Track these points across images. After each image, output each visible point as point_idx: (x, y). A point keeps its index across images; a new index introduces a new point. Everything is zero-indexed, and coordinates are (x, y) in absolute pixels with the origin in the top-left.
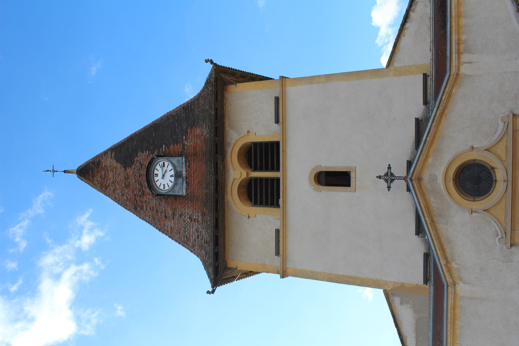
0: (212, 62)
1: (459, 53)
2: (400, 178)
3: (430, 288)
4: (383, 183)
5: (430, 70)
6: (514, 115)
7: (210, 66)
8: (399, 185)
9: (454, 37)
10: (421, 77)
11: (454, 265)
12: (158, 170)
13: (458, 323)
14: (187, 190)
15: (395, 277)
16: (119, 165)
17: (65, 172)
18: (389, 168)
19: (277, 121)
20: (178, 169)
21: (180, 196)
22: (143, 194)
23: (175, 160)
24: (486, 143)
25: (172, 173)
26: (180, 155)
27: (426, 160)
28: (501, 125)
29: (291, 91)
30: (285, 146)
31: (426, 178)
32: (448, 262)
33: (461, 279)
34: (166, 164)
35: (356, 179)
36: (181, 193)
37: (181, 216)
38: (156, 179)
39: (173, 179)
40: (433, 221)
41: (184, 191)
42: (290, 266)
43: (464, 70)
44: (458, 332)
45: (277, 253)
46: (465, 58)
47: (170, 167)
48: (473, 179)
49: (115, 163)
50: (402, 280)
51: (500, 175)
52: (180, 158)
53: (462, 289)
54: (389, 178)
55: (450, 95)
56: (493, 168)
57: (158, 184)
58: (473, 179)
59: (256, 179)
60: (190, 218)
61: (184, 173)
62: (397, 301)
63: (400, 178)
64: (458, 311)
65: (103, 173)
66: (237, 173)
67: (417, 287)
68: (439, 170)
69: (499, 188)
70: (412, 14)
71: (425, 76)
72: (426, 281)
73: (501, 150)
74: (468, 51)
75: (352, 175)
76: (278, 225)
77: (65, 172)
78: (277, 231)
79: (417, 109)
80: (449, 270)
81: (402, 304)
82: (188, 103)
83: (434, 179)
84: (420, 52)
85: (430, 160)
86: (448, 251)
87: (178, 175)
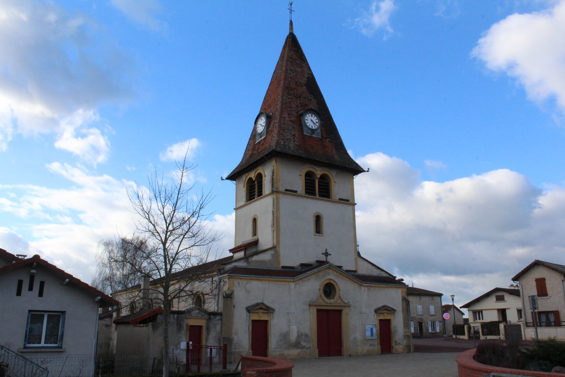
0: (368, 171)
1: (368, 286)
2: (326, 259)
3: (279, 268)
4: (329, 252)
5: (357, 273)
6: (349, 306)
7: (366, 170)
8: (323, 258)
9: (373, 285)
10: (354, 269)
11: (300, 282)
12: (315, 119)
13: (280, 283)
14: (307, 136)
15: (283, 251)
16: (306, 80)
17: (291, 21)
18: (330, 255)
19: (340, 199)
20: (315, 132)
21: (302, 129)
22: (297, 98)
23: (319, 131)
24: (341, 296)
25: (314, 128)
26: (322, 136)
27: (335, 271)
28: (346, 301)
29: (350, 207)
30: (328, 201)
31: (330, 271)
32: (301, 279)
33: (296, 284)
34: (317, 124)
35: (319, 237)
36: (304, 131)
37: (293, 127)
38: (310, 115)
39: (310, 127)
40: (315, 273)
41: (305, 134)
42: (281, 196)
43: (363, 288)
44: (276, 283)
45: (287, 190)
46: (366, 288)
47: (316, 127)
48: (329, 290)
49: (306, 76)
50: (281, 255)
51: (332, 301)
52: (320, 134)
53: (292, 285)
54: (326, 254)
55: (355, 282)
56: (333, 298)
57: (308, 115)
58: (329, 290)
59: (314, 181)
60: (294, 135)
61: (314, 136)
62: (272, 252)
63: (326, 259)
64: (284, 283)
65: (298, 62)
66: (319, 172)
67: (279, 262)
68: (332, 276)
69: (327, 301)
70: (374, 267)
71: (355, 271)
72: (283, 267)
73: (339, 301)
74: (368, 289)
75: (320, 235)
76: (299, 192)
77: (291, 21)
78: (296, 192)
79: (345, 268)
80: (299, 280)
81: (272, 254)
82: (344, 146)
83: (329, 274)
84: (364, 270)
85: (335, 273)
86: (305, 279)
87: (313, 131)
